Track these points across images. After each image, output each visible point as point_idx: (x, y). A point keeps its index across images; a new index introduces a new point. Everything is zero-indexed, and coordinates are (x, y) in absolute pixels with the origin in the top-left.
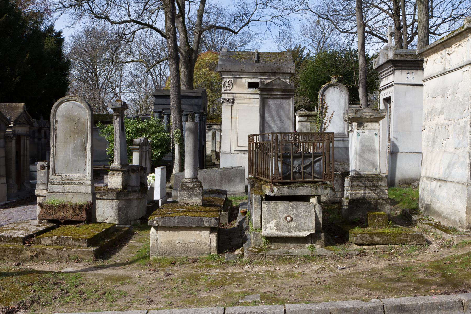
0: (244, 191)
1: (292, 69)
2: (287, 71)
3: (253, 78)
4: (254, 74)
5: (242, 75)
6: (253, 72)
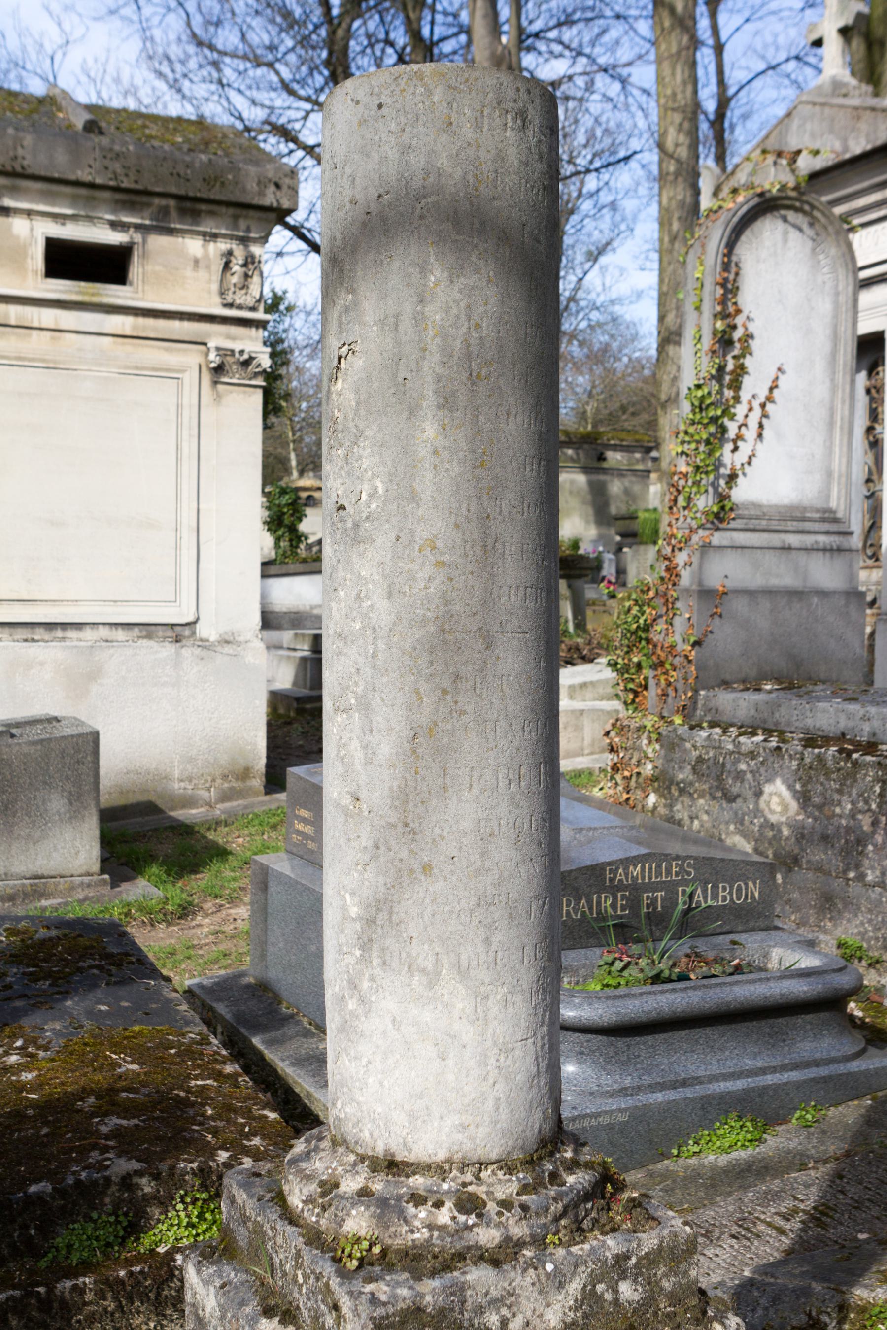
0: (96, 867)
1: (285, 188)
2: (262, 194)
3: (74, 218)
4: (83, 191)
5: (14, 191)
6: (77, 184)
